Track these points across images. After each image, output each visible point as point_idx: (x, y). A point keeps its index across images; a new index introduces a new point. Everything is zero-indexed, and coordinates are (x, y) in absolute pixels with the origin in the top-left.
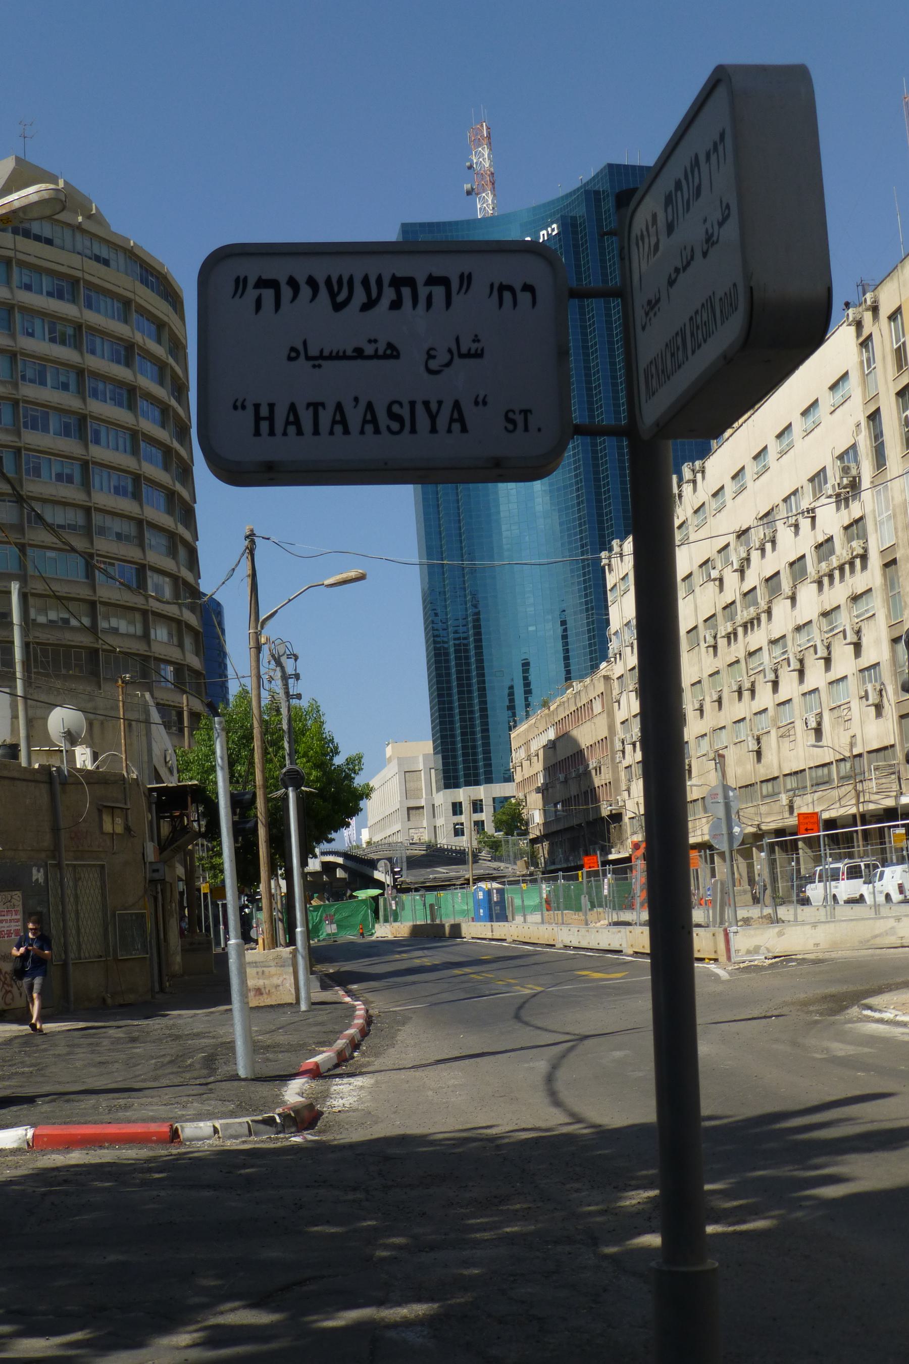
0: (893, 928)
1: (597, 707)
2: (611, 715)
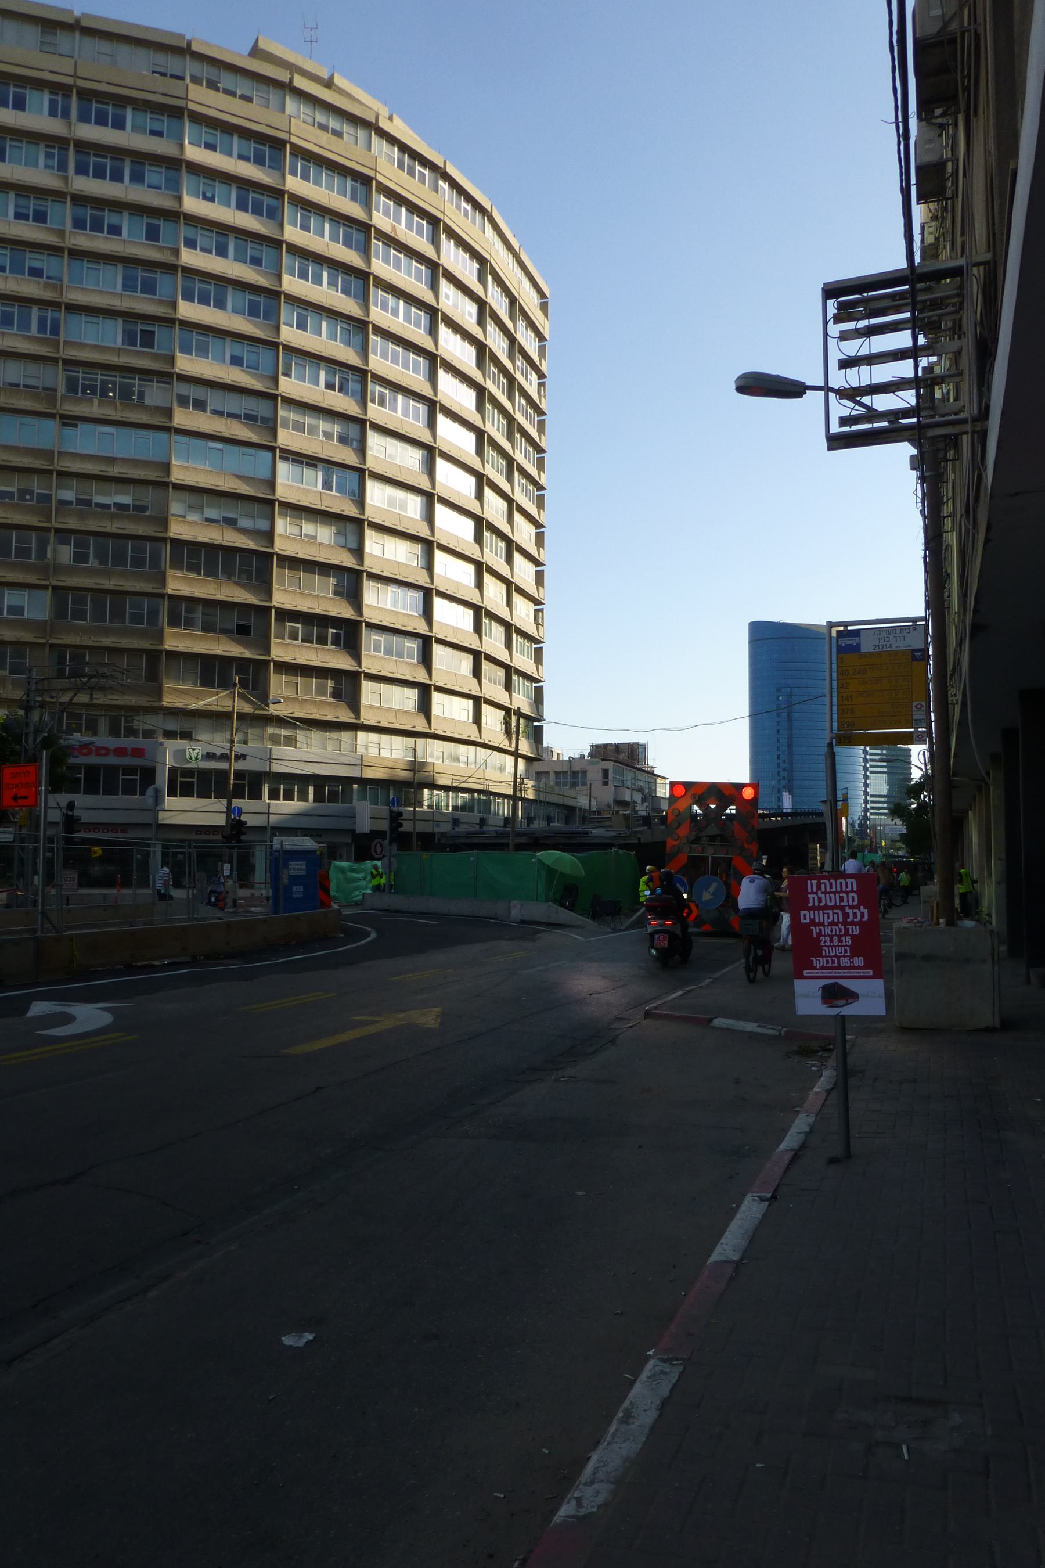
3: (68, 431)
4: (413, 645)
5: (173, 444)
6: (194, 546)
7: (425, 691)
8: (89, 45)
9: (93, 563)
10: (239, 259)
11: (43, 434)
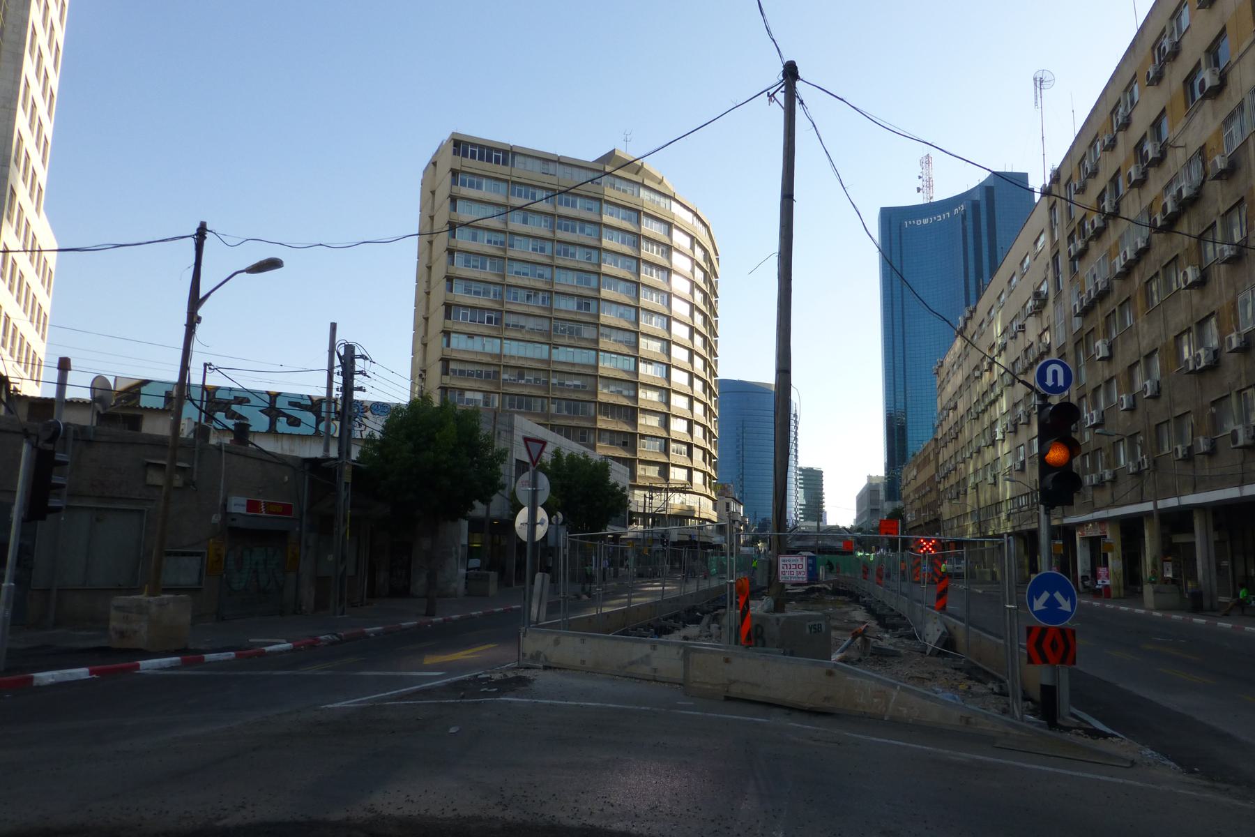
0: (648, 656)
3: (554, 351)
4: (684, 448)
5: (601, 358)
7: (690, 470)
8: (560, 168)
9: (565, 413)
10: (623, 267)
11: (541, 352)
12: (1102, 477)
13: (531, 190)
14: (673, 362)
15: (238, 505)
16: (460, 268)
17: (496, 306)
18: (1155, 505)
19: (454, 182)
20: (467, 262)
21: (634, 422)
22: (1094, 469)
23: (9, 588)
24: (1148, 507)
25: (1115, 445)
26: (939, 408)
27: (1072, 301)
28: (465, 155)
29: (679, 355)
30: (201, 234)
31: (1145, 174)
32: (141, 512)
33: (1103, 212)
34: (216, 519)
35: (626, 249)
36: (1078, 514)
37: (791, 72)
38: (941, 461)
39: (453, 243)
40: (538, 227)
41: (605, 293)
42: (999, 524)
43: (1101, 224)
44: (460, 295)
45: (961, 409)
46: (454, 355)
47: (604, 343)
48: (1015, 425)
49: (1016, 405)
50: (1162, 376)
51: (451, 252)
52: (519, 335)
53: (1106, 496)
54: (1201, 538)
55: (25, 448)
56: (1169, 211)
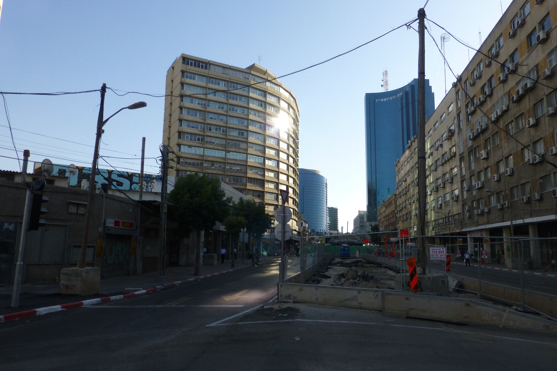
1: (393, 202)
2: (396, 204)
3: (228, 154)
6: (251, 178)
8: (231, 71)
9: (233, 182)
11: (221, 154)
12: (483, 211)
13: (217, 81)
14: (280, 160)
15: (110, 223)
16: (185, 115)
17: (202, 133)
18: (512, 223)
19: (183, 76)
20: (188, 113)
21: (263, 186)
22: (478, 207)
23: (20, 265)
24: (508, 223)
25: (489, 197)
26: (397, 181)
27: (467, 133)
28: (188, 64)
29: (283, 156)
30: (104, 89)
31: (507, 77)
32: (66, 226)
33: (485, 93)
34: (101, 229)
35: (260, 108)
36: (470, 226)
37: (422, 14)
38: (398, 204)
39: (182, 104)
40: (220, 97)
41: (251, 128)
42: (428, 232)
43: (484, 100)
44: (185, 128)
45: (409, 181)
46: (183, 155)
47: (250, 151)
48: (437, 188)
49: (437, 179)
50: (514, 166)
51: (181, 108)
52: (212, 147)
53: (485, 219)
54: (532, 237)
55: (28, 193)
56: (520, 93)
